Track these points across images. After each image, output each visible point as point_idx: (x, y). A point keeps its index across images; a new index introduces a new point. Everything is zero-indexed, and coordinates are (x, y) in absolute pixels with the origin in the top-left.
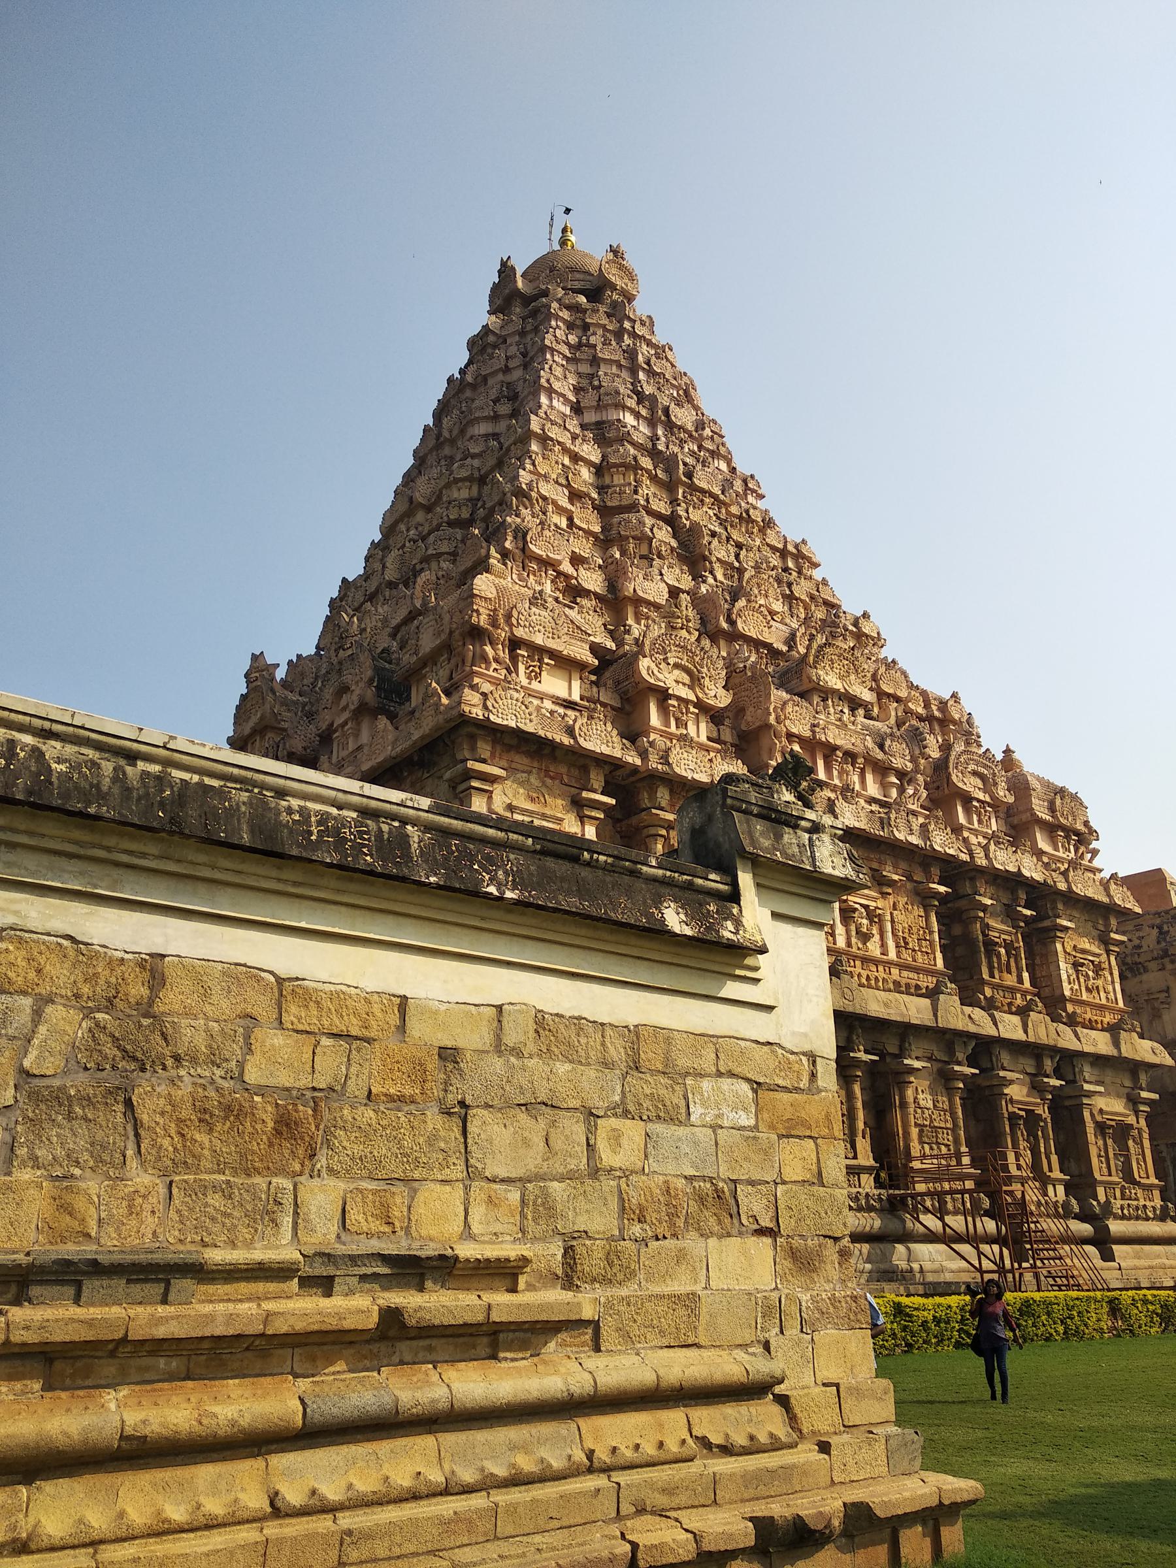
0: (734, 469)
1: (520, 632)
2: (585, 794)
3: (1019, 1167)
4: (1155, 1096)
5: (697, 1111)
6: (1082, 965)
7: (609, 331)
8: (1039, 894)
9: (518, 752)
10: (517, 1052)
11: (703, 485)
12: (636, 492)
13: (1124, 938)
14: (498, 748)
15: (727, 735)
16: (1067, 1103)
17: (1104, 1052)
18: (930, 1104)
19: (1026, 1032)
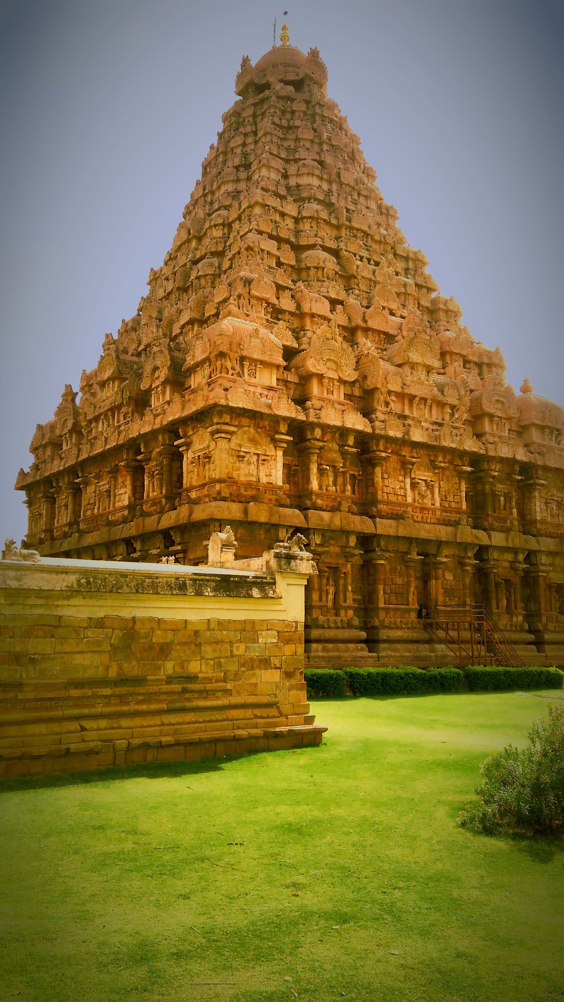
1: (245, 353)
2: (277, 436)
5: (260, 640)
9: (244, 417)
10: (213, 630)
16: (532, 575)
19: (507, 541)
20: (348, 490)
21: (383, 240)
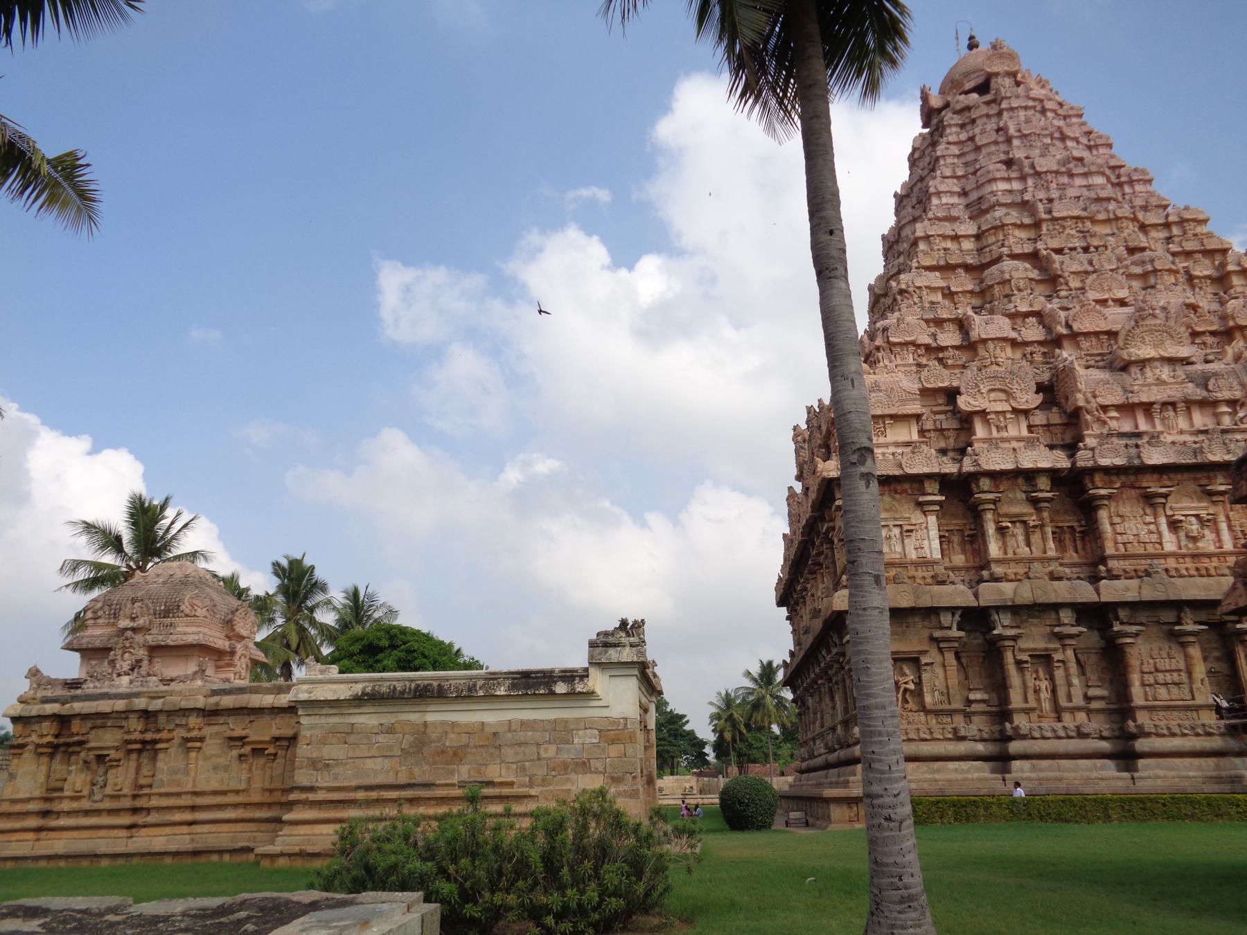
20: (1050, 549)
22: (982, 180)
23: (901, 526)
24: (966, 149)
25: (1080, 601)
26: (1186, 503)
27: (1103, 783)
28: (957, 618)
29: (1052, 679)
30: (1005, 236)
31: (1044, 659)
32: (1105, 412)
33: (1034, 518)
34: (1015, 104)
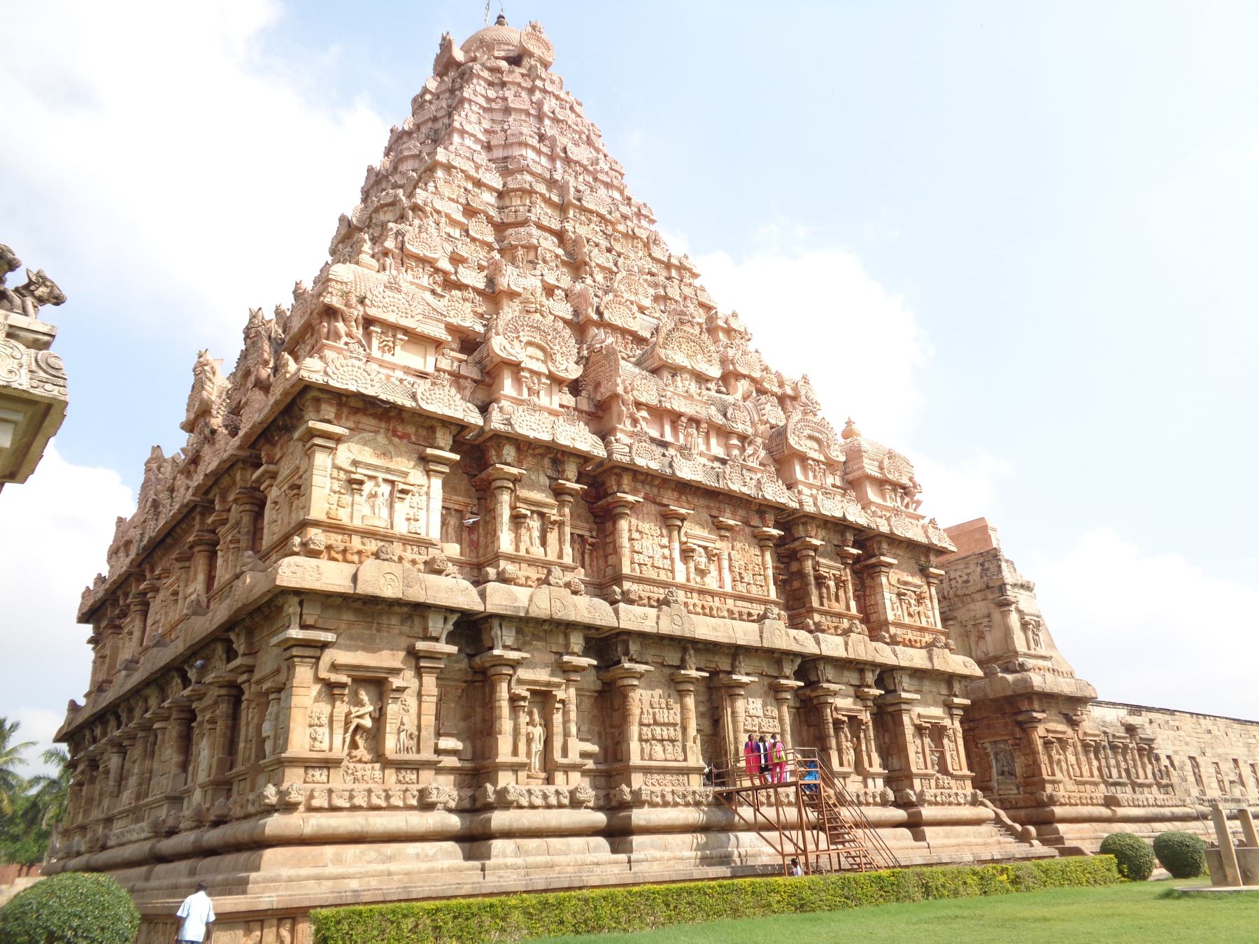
0: (629, 199)
1: (373, 312)
3: (841, 764)
4: (967, 702)
6: (905, 594)
7: (523, 88)
8: (866, 538)
9: (365, 414)
11: (591, 206)
12: (529, 211)
13: (942, 572)
14: (345, 411)
15: (585, 406)
16: (891, 709)
17: (918, 666)
18: (760, 713)
21: (630, 232)
22: (511, 140)
23: (392, 483)
24: (494, 105)
25: (598, 623)
26: (698, 531)
27: (598, 870)
28: (450, 627)
29: (547, 725)
30: (531, 202)
31: (543, 697)
32: (638, 410)
33: (555, 511)
34: (549, 88)
